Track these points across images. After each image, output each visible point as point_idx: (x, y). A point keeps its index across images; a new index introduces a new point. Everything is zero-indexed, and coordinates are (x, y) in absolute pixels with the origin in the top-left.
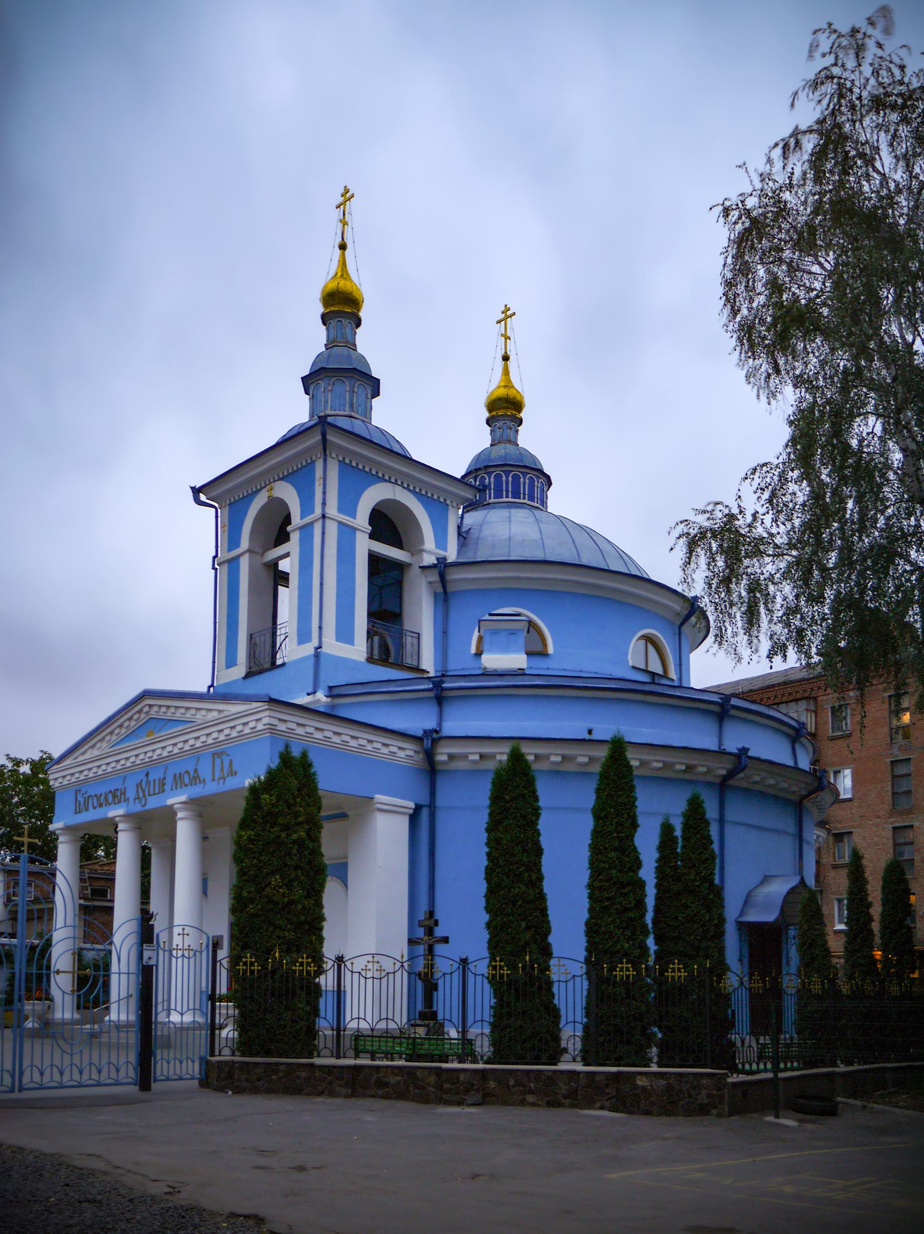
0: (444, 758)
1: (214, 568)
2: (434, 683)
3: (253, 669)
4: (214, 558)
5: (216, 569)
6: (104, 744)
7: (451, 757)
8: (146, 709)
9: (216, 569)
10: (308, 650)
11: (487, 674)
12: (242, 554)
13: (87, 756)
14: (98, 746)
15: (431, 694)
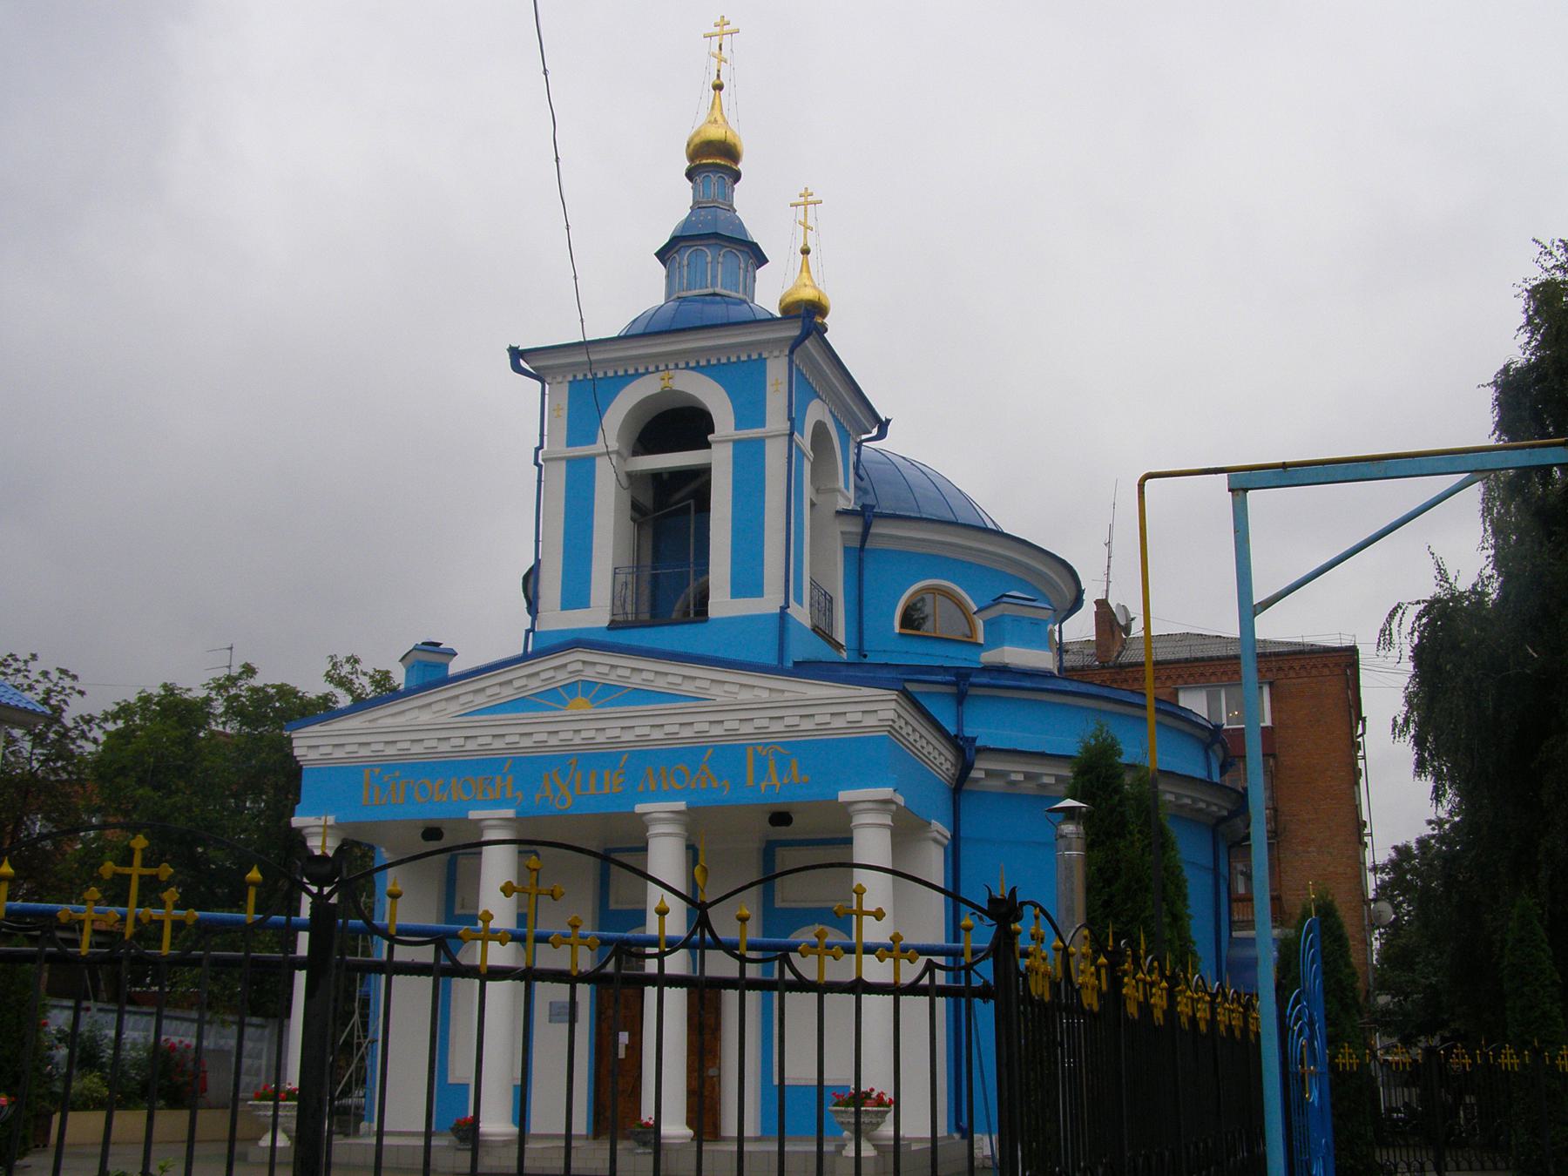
0: (982, 775)
1: (536, 463)
2: (956, 675)
3: (617, 618)
4: (537, 450)
5: (540, 467)
6: (454, 707)
7: (989, 773)
8: (579, 666)
9: (540, 467)
10: (769, 603)
11: (1003, 670)
12: (600, 455)
13: (401, 720)
14: (435, 708)
15: (953, 690)
